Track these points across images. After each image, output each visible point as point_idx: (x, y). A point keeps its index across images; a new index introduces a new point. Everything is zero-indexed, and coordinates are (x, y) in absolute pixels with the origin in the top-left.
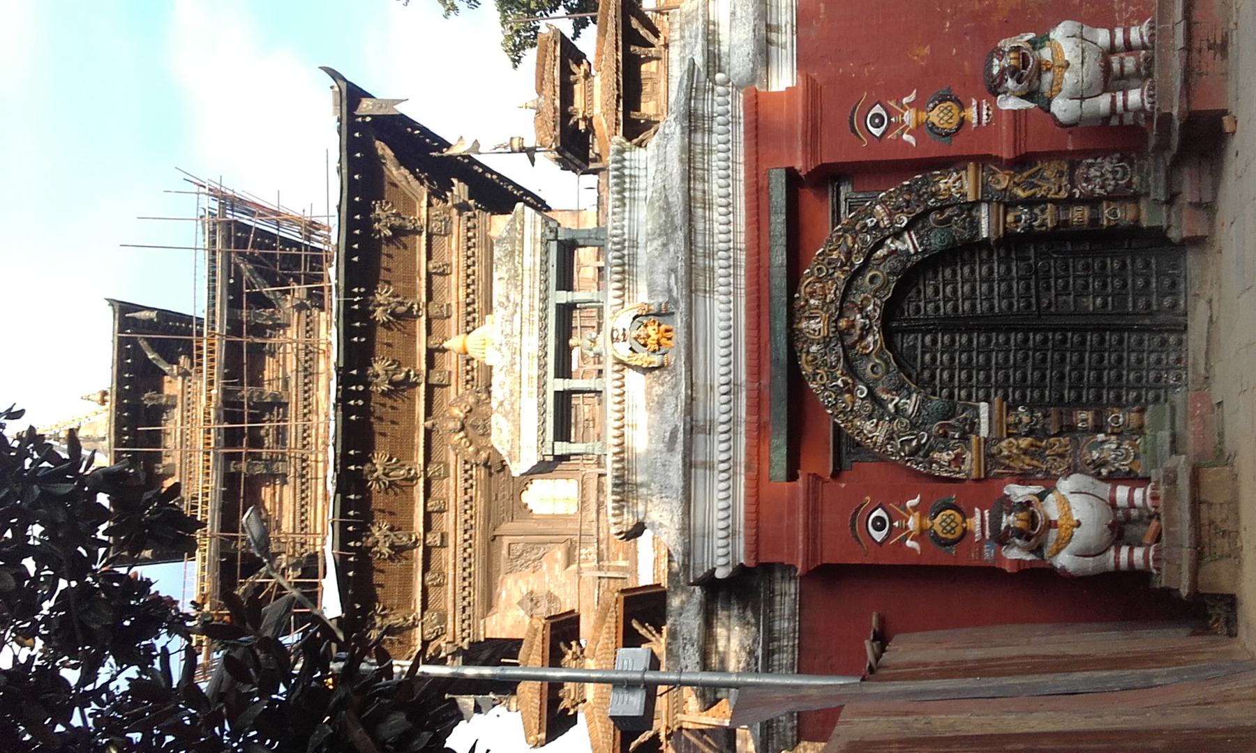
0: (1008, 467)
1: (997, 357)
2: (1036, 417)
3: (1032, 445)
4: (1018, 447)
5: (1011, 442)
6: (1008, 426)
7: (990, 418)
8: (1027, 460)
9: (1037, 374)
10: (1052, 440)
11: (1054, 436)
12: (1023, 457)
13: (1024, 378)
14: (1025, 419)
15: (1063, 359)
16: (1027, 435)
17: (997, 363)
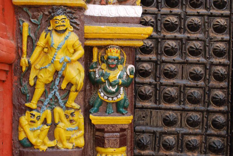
0: (32, 44)
1: (198, 39)
2: (118, 91)
3: (70, 85)
4: (67, 63)
5: (75, 51)
6: (105, 48)
7: (117, 20)
8: (46, 77)
9: (173, 91)
10: (80, 117)
11: (88, 122)
12: (51, 69)
13: (169, 75)
14: (115, 75)
15: (193, 124)
16: (89, 78)
17: (189, 39)
